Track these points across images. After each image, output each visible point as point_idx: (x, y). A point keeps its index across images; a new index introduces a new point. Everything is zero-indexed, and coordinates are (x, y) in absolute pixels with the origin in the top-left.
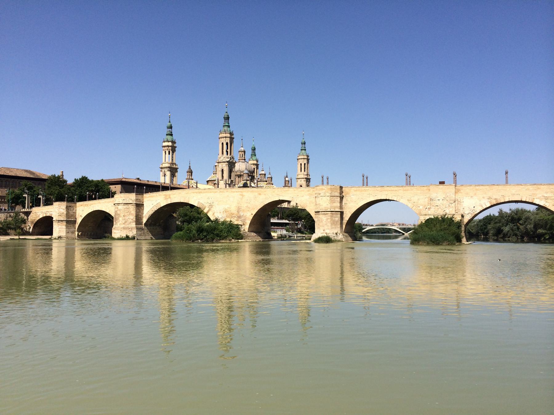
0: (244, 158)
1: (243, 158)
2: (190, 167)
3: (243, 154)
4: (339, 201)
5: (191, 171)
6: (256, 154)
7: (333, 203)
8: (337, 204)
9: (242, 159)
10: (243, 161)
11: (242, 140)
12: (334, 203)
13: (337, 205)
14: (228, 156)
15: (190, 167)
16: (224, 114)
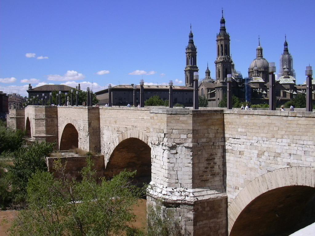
0: (261, 55)
1: (260, 56)
2: (208, 68)
3: (260, 52)
4: (45, 124)
5: (209, 71)
6: (288, 49)
7: (38, 126)
8: (43, 128)
9: (259, 57)
10: (260, 58)
11: (259, 38)
12: (40, 126)
13: (42, 129)
14: (222, 57)
15: (208, 68)
16: (220, 18)
